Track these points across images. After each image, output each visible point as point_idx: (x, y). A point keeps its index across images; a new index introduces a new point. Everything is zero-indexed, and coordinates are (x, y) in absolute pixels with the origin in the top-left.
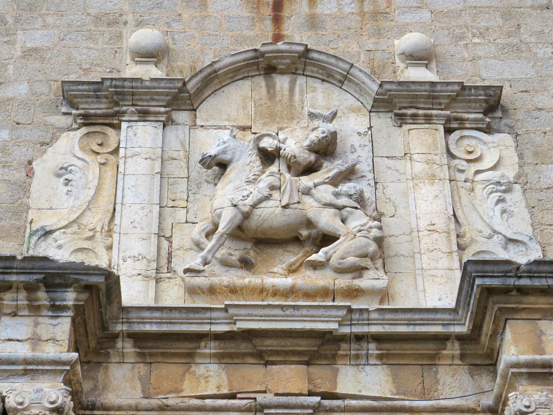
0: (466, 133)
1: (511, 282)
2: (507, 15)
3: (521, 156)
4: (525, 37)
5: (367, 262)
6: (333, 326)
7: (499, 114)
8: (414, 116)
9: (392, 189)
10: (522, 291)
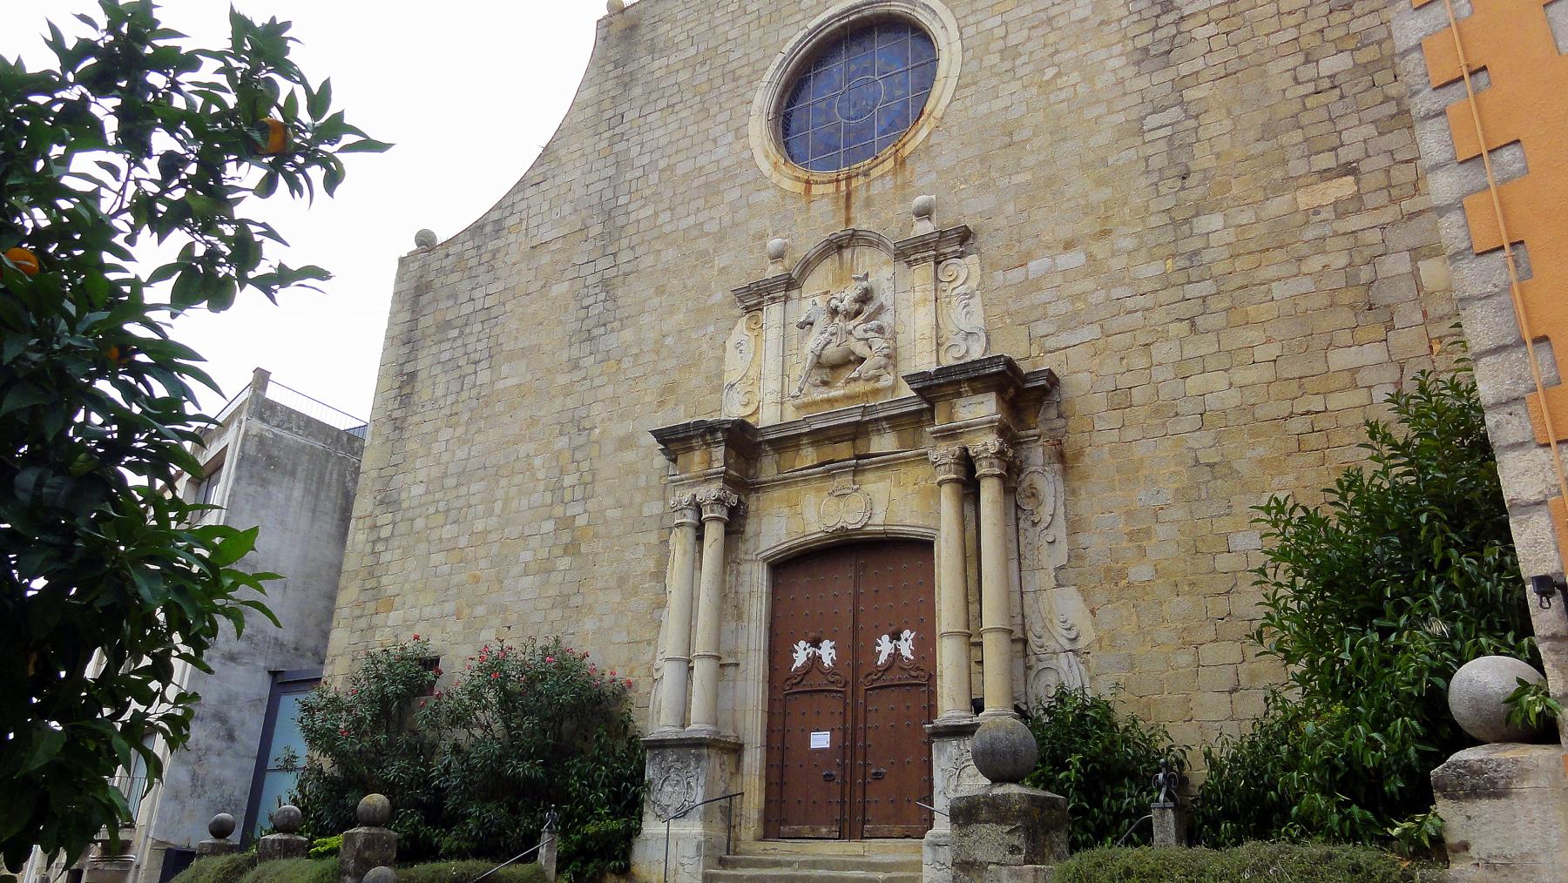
2: (983, 161)
3: (982, 269)
4: (994, 174)
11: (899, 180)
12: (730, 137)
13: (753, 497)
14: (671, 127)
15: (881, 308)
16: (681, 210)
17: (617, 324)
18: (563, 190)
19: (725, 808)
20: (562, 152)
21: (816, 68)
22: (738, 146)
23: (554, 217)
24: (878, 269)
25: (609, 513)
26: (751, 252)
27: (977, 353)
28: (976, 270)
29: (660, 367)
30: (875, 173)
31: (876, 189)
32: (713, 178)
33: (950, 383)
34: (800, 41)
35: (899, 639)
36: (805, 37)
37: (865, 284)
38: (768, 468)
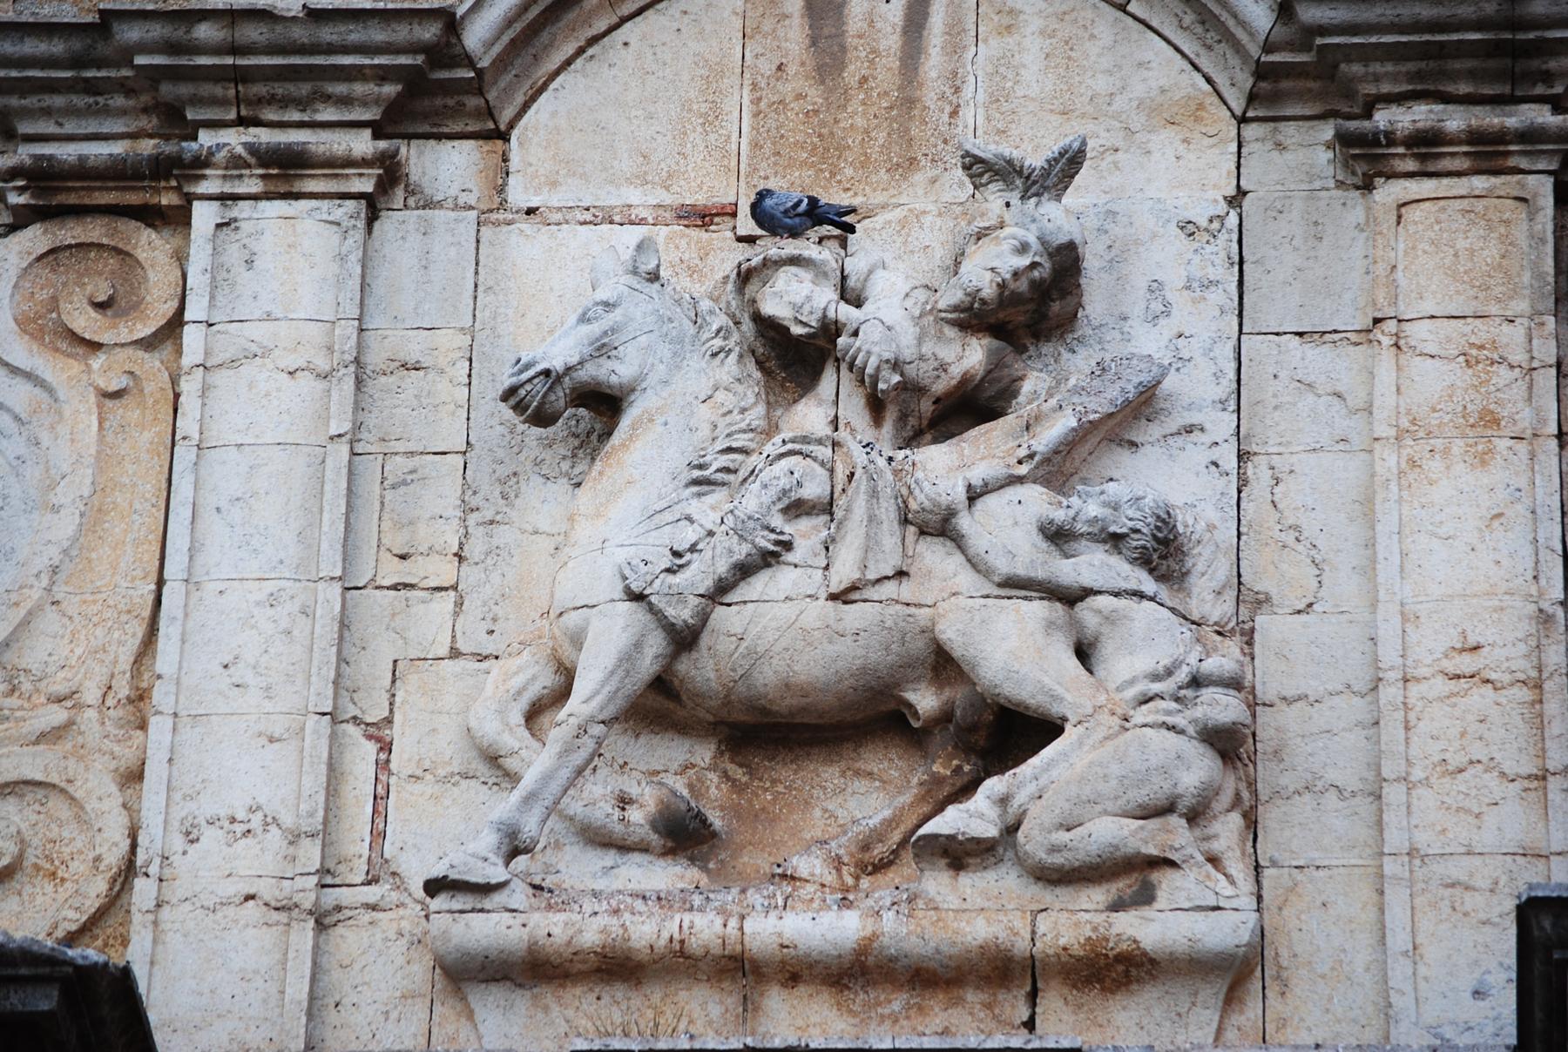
5: (1176, 835)
8: (1426, 143)
9: (1313, 482)
15: (1134, 415)
37: (1059, 217)
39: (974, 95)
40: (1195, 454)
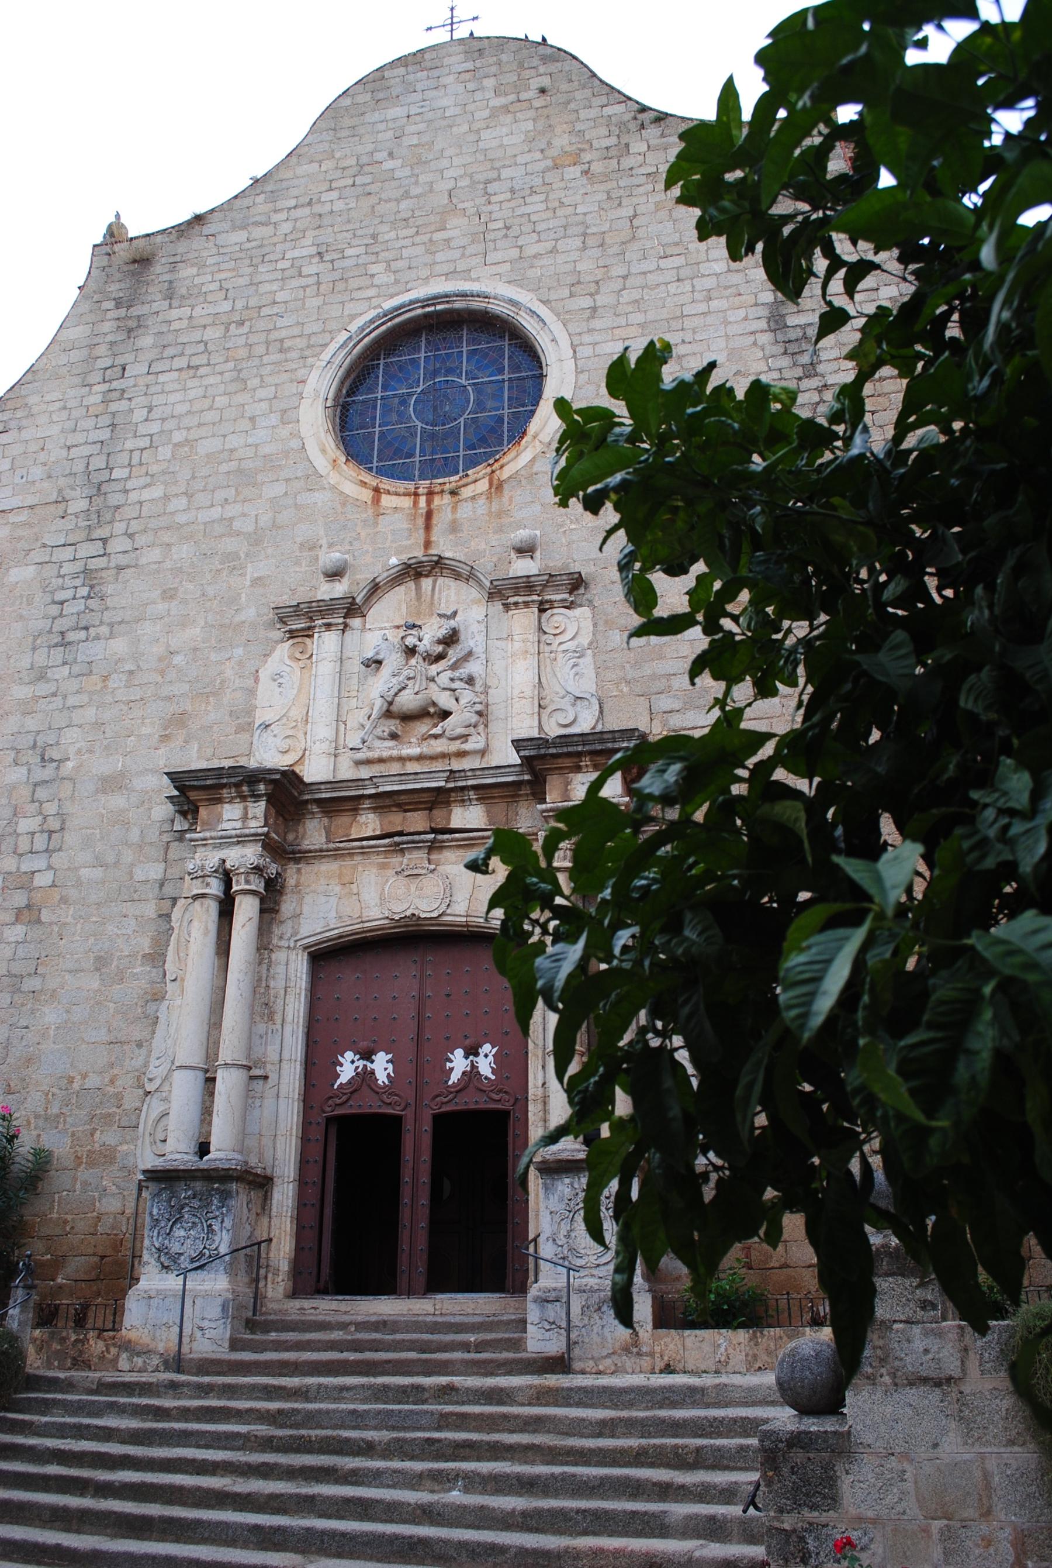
0: (555, 611)
1: (542, 752)
3: (595, 625)
5: (472, 730)
6: (442, 784)
7: (582, 591)
8: (516, 604)
9: (498, 666)
10: (553, 756)
11: (495, 507)
12: (274, 419)
13: (291, 869)
14: (192, 394)
16: (202, 499)
17: (104, 630)
18: (33, 447)
19: (251, 1257)
20: (33, 400)
21: (387, 355)
22: (284, 432)
23: (17, 480)
24: (463, 605)
25: (84, 872)
26: (298, 563)
27: (585, 725)
28: (587, 626)
29: (165, 691)
30: (466, 492)
31: (465, 511)
32: (248, 464)
33: (569, 755)
34: (372, 321)
35: (477, 1054)
36: (378, 317)
37: (452, 623)
38: (314, 833)
39: (443, 600)
40: (479, 662)
